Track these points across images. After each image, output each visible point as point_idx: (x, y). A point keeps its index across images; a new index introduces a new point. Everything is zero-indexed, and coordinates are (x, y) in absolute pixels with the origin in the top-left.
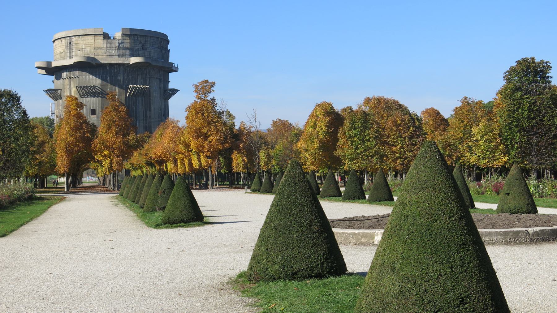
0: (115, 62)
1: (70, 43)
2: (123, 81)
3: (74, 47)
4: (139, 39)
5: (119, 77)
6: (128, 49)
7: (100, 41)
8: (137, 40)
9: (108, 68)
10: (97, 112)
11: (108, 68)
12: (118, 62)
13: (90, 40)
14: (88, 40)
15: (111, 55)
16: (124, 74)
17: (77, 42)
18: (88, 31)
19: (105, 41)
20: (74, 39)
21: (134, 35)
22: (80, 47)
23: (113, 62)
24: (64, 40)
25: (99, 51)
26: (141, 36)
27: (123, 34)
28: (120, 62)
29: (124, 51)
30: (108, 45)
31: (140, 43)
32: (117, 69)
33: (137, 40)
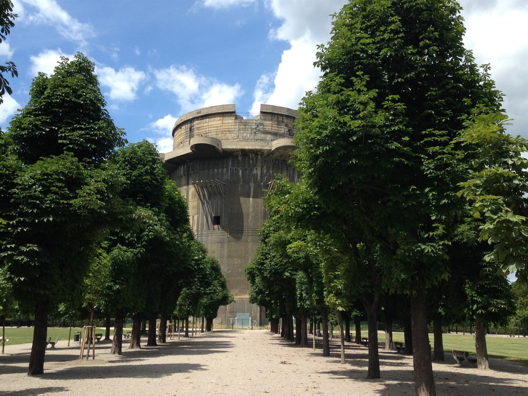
0: (250, 148)
1: (190, 130)
2: (261, 177)
3: (196, 132)
4: (285, 121)
5: (255, 172)
6: (269, 133)
7: (230, 121)
8: (283, 122)
9: (240, 158)
10: (222, 220)
11: (240, 158)
12: (254, 148)
13: (216, 122)
14: (214, 121)
15: (245, 140)
16: (262, 166)
17: (199, 126)
18: (214, 109)
19: (237, 121)
20: (196, 122)
21: (278, 114)
22: (202, 131)
23: (247, 148)
24: (183, 127)
25: (229, 136)
26: (287, 116)
27: (262, 112)
28: (257, 148)
29: (263, 136)
30: (242, 127)
31: (286, 126)
32: (253, 159)
33: (283, 122)
